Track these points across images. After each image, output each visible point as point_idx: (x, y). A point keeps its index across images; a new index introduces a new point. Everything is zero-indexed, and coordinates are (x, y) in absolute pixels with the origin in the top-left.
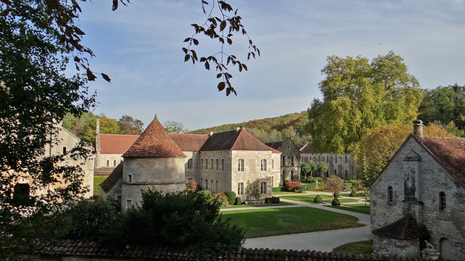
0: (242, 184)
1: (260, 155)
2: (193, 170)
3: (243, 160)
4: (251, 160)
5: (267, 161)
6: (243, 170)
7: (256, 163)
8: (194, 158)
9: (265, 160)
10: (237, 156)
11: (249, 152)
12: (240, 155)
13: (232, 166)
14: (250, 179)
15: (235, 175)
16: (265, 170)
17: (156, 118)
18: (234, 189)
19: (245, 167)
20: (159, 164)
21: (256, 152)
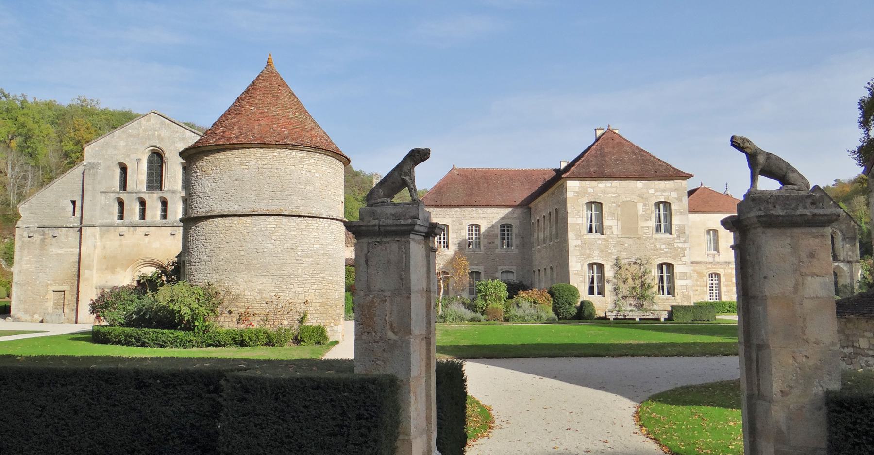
0: (601, 267)
1: (651, 191)
2: (514, 250)
3: (599, 205)
4: (625, 203)
5: (673, 207)
6: (600, 230)
7: (640, 212)
8: (515, 223)
9: (667, 205)
10: (581, 193)
11: (616, 183)
12: (590, 190)
14: (624, 254)
15: (579, 242)
16: (669, 230)
17: (269, 64)
18: (578, 278)
19: (606, 223)
20: (242, 164)
21: (640, 184)
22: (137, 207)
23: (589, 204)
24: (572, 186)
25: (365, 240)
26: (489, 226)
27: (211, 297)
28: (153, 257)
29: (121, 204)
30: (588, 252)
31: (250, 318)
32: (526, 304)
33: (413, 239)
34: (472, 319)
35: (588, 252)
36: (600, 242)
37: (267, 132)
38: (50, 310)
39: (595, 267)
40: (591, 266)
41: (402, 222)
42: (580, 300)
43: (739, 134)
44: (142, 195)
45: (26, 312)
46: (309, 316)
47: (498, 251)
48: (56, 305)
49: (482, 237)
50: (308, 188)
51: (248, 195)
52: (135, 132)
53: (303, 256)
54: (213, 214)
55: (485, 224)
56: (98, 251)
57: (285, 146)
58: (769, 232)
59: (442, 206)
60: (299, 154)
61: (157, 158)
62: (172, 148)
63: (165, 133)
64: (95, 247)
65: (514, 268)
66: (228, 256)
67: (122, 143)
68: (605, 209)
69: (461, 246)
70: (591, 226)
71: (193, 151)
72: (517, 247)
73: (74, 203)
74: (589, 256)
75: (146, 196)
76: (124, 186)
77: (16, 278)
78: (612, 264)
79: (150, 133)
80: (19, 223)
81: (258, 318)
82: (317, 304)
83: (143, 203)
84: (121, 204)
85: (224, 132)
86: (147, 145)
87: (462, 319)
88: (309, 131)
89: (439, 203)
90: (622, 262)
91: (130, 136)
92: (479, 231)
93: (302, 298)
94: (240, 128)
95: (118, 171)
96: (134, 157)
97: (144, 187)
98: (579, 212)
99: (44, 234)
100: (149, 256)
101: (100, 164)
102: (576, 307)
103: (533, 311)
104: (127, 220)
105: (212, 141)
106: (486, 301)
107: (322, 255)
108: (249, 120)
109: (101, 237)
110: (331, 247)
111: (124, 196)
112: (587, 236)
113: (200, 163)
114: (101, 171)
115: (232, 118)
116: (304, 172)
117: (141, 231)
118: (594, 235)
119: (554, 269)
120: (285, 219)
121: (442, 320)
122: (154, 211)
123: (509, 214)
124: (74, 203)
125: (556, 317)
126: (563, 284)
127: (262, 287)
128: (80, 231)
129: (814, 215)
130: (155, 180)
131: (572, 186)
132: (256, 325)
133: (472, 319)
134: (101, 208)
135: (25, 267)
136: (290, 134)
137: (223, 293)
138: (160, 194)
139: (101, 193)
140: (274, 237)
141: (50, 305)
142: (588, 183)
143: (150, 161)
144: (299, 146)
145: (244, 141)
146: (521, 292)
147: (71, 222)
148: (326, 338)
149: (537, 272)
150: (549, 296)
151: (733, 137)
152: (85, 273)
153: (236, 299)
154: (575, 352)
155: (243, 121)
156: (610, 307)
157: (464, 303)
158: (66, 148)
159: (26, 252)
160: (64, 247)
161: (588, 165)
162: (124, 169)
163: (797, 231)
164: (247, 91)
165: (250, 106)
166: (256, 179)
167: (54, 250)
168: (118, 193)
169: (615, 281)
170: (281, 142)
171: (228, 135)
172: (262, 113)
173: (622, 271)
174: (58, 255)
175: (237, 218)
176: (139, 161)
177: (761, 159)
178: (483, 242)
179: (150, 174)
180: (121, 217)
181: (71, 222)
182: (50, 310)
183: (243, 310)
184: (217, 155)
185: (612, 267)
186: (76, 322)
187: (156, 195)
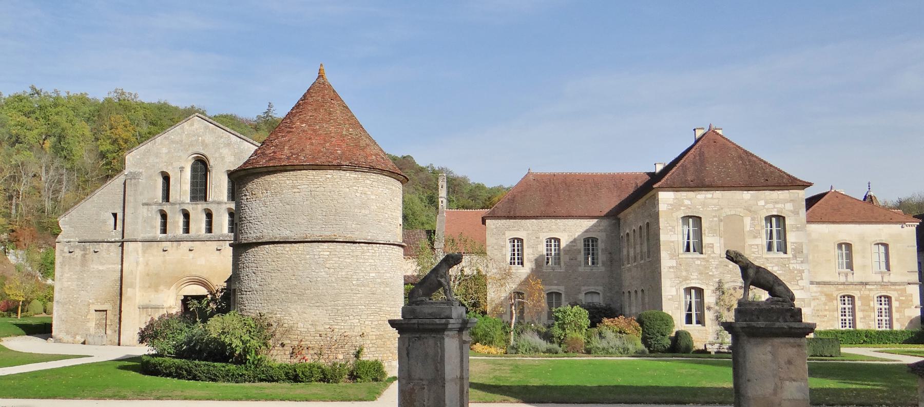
0: (700, 292)
2: (600, 268)
6: (699, 248)
8: (601, 236)
10: (675, 207)
12: (687, 202)
13: (663, 237)
18: (673, 304)
19: (706, 240)
20: (293, 187)
22: (181, 219)
23: (686, 218)
24: (666, 198)
25: (406, 336)
26: (571, 240)
27: (262, 329)
28: (198, 274)
29: (164, 216)
30: (684, 274)
31: (303, 352)
32: (609, 334)
33: (448, 336)
34: (549, 351)
35: (684, 274)
36: (698, 262)
37: (319, 152)
38: (92, 331)
39: (693, 291)
40: (688, 290)
41: (437, 321)
42: (675, 330)
43: (732, 249)
44: (185, 207)
45: (68, 333)
46: (365, 350)
47: (581, 269)
48: (98, 326)
49: (562, 253)
50: (363, 211)
51: (299, 220)
52: (177, 138)
53: (358, 285)
54: (264, 240)
55: (566, 237)
56: (141, 268)
57: (339, 167)
58: (752, 340)
59: (515, 218)
60: (354, 175)
61: (201, 167)
62: (217, 155)
63: (209, 139)
64: (137, 263)
65: (600, 289)
66: (280, 285)
67: (164, 150)
68: (705, 224)
69: (540, 263)
70: (688, 244)
71: (242, 173)
72: (603, 264)
73: (115, 215)
74: (686, 279)
75: (190, 208)
76: (166, 197)
77: (57, 296)
78: (713, 288)
79: (194, 139)
80: (60, 238)
81: (312, 352)
82: (374, 337)
83: (186, 215)
84: (164, 216)
85: (274, 152)
86: (190, 152)
87: (536, 350)
88: (363, 149)
89: (512, 214)
90: (726, 286)
91: (173, 142)
92: (559, 246)
93: (358, 331)
94: (291, 148)
95: (160, 181)
96: (177, 165)
97: (187, 198)
98: (673, 227)
99: (85, 249)
100: (194, 274)
101: (141, 173)
102: (670, 338)
103: (618, 343)
104: (170, 234)
105: (263, 162)
106: (564, 329)
107: (379, 283)
108: (301, 138)
109: (144, 252)
110: (388, 275)
111: (167, 208)
112: (684, 256)
113: (250, 186)
114: (142, 181)
115: (283, 137)
116: (358, 195)
117: (186, 246)
118: (692, 255)
119: (646, 292)
120: (339, 246)
121: (514, 351)
122: (198, 224)
123: (594, 226)
124: (115, 215)
125: (647, 350)
126: (654, 311)
127: (316, 318)
128: (122, 246)
129: (791, 328)
130: (200, 190)
131: (666, 198)
132: (310, 361)
133: (549, 351)
134: (142, 221)
135: (66, 284)
136: (343, 153)
137: (275, 325)
138: (205, 206)
139: (144, 204)
140: (328, 266)
141: (92, 325)
142: (684, 194)
143: (194, 169)
144: (354, 167)
145: (296, 162)
146: (605, 320)
147: (112, 237)
148: (383, 374)
149: (627, 294)
150: (638, 324)
151: (728, 251)
152: (127, 292)
153: (288, 331)
154: (657, 398)
155: (294, 139)
156: (711, 338)
157: (539, 333)
158: (102, 148)
159: (67, 268)
160: (105, 262)
161: (685, 173)
162: (166, 178)
163: (777, 341)
164: (298, 105)
165: (302, 123)
166: (308, 202)
167: (95, 266)
168: (160, 204)
169: (717, 308)
170: (335, 163)
171: (278, 155)
172: (314, 131)
173: (726, 297)
174: (99, 271)
175: (289, 245)
176: (182, 169)
177: (751, 272)
178: (564, 258)
179: (193, 184)
180: (164, 231)
181: (112, 237)
182: (92, 331)
183: (296, 343)
184: (267, 178)
185: (714, 292)
186: (119, 345)
187: (201, 206)
